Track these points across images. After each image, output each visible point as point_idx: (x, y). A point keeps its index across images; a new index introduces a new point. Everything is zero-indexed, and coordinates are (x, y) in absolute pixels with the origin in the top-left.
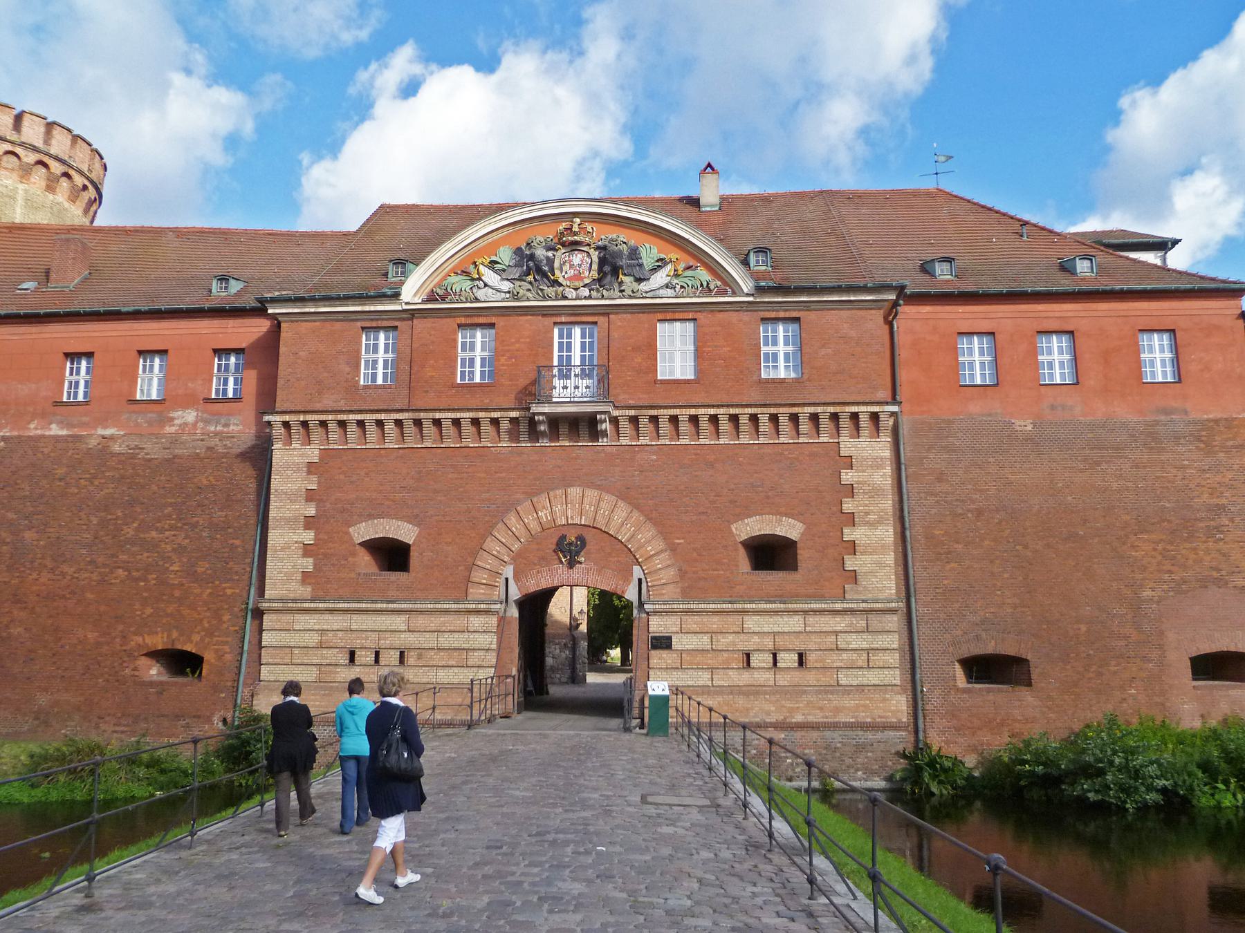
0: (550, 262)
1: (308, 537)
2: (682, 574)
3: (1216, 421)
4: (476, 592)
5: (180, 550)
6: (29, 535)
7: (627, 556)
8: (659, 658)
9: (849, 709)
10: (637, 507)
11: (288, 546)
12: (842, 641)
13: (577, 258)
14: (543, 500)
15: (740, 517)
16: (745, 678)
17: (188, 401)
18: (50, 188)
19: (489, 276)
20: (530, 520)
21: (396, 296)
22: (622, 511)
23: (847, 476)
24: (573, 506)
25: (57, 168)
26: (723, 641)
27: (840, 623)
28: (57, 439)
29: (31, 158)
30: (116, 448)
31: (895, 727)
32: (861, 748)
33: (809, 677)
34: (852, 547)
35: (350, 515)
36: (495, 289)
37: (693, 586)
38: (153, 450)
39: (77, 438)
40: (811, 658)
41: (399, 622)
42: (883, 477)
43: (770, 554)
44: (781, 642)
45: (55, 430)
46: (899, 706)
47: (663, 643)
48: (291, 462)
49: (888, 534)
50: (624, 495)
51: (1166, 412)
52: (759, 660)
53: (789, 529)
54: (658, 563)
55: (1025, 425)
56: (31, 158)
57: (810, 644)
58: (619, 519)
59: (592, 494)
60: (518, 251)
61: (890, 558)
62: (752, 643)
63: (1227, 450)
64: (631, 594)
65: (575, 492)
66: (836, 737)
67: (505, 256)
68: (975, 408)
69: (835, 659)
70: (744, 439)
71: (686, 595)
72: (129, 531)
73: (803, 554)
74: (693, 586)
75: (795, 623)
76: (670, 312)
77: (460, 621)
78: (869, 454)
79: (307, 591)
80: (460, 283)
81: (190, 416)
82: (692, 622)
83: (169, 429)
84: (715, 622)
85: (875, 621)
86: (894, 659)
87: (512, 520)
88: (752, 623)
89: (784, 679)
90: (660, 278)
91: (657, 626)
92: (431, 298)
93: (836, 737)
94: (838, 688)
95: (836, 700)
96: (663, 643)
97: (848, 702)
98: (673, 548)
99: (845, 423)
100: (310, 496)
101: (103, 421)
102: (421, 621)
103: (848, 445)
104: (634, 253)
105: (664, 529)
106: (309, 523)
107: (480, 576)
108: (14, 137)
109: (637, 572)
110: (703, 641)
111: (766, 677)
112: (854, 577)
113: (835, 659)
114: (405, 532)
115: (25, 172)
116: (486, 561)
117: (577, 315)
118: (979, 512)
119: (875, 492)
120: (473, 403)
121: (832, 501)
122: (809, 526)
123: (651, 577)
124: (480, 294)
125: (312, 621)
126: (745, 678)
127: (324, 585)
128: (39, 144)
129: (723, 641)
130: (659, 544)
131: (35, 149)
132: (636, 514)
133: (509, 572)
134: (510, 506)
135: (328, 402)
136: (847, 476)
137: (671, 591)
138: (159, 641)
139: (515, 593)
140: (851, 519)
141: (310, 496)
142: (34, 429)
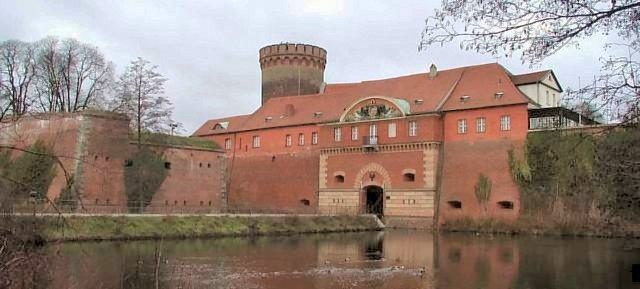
7: (381, 178)
8: (388, 201)
9: (422, 213)
11: (323, 176)
16: (402, 206)
18: (308, 64)
19: (357, 115)
23: (425, 159)
25: (308, 58)
27: (420, 193)
29: (301, 58)
32: (423, 222)
33: (416, 206)
35: (332, 172)
37: (394, 184)
38: (303, 156)
46: (432, 213)
47: (388, 198)
48: (323, 158)
50: (383, 165)
52: (407, 202)
53: (413, 172)
55: (472, 144)
56: (301, 58)
62: (404, 198)
67: (359, 110)
69: (422, 202)
74: (396, 187)
75: (413, 193)
76: (391, 121)
84: (398, 193)
86: (433, 202)
90: (389, 112)
91: (388, 194)
96: (388, 198)
103: (425, 152)
106: (326, 172)
110: (394, 198)
111: (407, 206)
113: (422, 202)
114: (343, 174)
115: (300, 62)
117: (374, 123)
123: (385, 184)
126: (402, 206)
131: (301, 55)
137: (390, 187)
138: (303, 198)
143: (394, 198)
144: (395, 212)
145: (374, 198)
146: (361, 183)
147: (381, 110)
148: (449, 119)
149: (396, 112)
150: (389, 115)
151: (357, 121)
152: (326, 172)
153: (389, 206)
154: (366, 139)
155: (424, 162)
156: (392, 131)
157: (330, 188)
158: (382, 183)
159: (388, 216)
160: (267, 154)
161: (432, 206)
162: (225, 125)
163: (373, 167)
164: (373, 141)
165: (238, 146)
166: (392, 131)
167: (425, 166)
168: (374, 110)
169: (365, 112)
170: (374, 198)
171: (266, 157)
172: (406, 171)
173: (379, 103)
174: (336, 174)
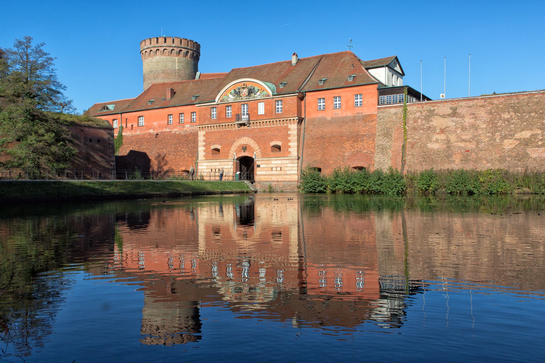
0: (239, 92)
1: (204, 148)
2: (262, 153)
3: (368, 115)
4: (230, 158)
5: (187, 152)
6: (164, 150)
8: (258, 169)
9: (288, 178)
10: (255, 140)
12: (288, 165)
13: (244, 91)
14: (239, 140)
15: (271, 141)
17: (187, 123)
19: (230, 96)
20: (238, 144)
21: (215, 102)
22: (252, 141)
23: (289, 132)
24: (245, 140)
26: (268, 166)
28: (168, 132)
30: (177, 133)
31: (295, 181)
32: (290, 185)
33: (282, 172)
34: (289, 147)
36: (231, 98)
38: (183, 133)
39: (171, 131)
40: (282, 168)
41: (218, 164)
42: (295, 132)
43: (279, 148)
44: (278, 165)
45: (168, 130)
47: (259, 166)
49: (296, 144)
51: (358, 113)
52: (274, 169)
53: (279, 143)
54: (258, 151)
55: (329, 118)
57: (282, 166)
58: (251, 142)
59: (247, 138)
60: (235, 90)
61: (296, 149)
63: (369, 121)
64: (254, 157)
65: (245, 138)
66: (285, 183)
67: (233, 91)
68: (320, 115)
70: (272, 126)
71: (262, 157)
72: (179, 149)
73: (282, 148)
74: (264, 155)
75: (280, 162)
76: (260, 100)
77: (227, 163)
78: (293, 127)
79: (204, 159)
80: (225, 97)
81: (188, 126)
82: (263, 162)
83: (185, 129)
84: (267, 162)
85: (293, 161)
86: (296, 168)
87: (235, 144)
88: (273, 162)
89: (278, 173)
90: (258, 93)
91: (258, 163)
92: (221, 101)
93: (285, 183)
94: (287, 174)
95: (286, 177)
96: (259, 166)
97: (288, 177)
98: (260, 148)
99: (288, 121)
100: (204, 141)
101: (175, 128)
102: (222, 163)
103: (290, 126)
104: (254, 89)
105: (259, 145)
107: (230, 155)
108: (174, 45)
109: (255, 153)
110: (265, 166)
111: (274, 172)
112: (290, 152)
114: (219, 147)
116: (231, 152)
118: (317, 138)
119: (294, 135)
120: (229, 121)
121: (286, 137)
122: (283, 143)
123: (256, 154)
124: (229, 100)
125: (205, 164)
127: (207, 158)
128: (179, 45)
129: (268, 166)
130: (258, 147)
132: (254, 142)
133: (235, 154)
134: (234, 141)
135: (206, 123)
136: (289, 132)
137: (260, 156)
138: (184, 169)
139: (236, 158)
140: (289, 141)
141: (204, 141)
142: (164, 130)
143: (265, 166)
144: (263, 178)
145: (246, 165)
146: (234, 154)
147: (251, 92)
148: (309, 97)
149: (265, 93)
150: (258, 95)
151: (230, 100)
152: (204, 146)
153: (260, 174)
154: (238, 117)
155: (289, 135)
156: (261, 109)
157: (207, 158)
158: (253, 153)
159: (259, 182)
160: (151, 131)
161: (296, 172)
162: (111, 107)
163: (245, 140)
164: (245, 118)
165: (124, 125)
166: (261, 109)
167: (289, 138)
168: (245, 91)
169: (237, 93)
170: (246, 165)
171: (150, 134)
172: (273, 143)
173: (249, 86)
174: (213, 147)
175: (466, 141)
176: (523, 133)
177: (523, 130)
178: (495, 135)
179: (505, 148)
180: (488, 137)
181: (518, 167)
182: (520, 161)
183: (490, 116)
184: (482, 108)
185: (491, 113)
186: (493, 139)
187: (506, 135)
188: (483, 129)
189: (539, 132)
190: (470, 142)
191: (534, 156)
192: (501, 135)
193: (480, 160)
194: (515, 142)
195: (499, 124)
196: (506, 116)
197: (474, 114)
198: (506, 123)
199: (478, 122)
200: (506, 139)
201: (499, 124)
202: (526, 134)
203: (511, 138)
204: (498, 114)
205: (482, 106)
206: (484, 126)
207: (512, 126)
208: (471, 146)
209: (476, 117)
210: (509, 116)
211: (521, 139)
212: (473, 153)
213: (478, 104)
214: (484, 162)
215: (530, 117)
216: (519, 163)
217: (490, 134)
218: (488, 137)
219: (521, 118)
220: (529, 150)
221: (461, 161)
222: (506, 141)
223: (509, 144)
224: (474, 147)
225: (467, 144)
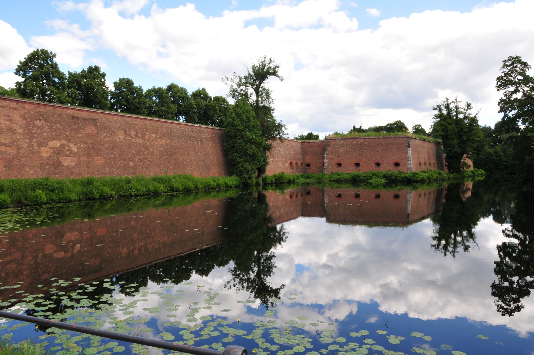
175: (6, 146)
176: (54, 142)
177: (54, 139)
178: (32, 142)
179: (43, 155)
180: (27, 143)
181: (55, 174)
182: (56, 168)
183: (25, 121)
184: (15, 111)
185: (25, 118)
186: (31, 145)
187: (41, 143)
188: (20, 134)
189: (66, 143)
190: (10, 146)
191: (66, 164)
192: (37, 142)
193: (23, 166)
194: (50, 150)
195: (34, 131)
196: (38, 123)
197: (9, 116)
198: (40, 130)
199: (15, 126)
200: (42, 146)
201: (34, 131)
202: (57, 144)
203: (46, 146)
204: (32, 121)
205: (15, 109)
206: (21, 131)
207: (45, 134)
208: (12, 151)
209: (11, 120)
210: (41, 124)
211: (53, 148)
212: (15, 160)
213: (11, 106)
214: (27, 169)
215: (57, 127)
216: (56, 171)
217: (27, 140)
218: (27, 143)
219: (50, 128)
220: (62, 159)
221: (5, 167)
222: (42, 148)
223: (45, 152)
224: (15, 152)
225: (8, 148)
